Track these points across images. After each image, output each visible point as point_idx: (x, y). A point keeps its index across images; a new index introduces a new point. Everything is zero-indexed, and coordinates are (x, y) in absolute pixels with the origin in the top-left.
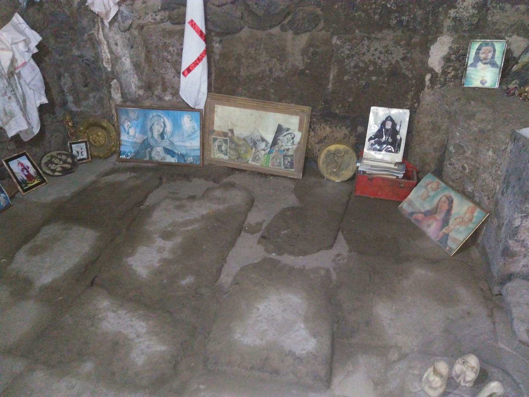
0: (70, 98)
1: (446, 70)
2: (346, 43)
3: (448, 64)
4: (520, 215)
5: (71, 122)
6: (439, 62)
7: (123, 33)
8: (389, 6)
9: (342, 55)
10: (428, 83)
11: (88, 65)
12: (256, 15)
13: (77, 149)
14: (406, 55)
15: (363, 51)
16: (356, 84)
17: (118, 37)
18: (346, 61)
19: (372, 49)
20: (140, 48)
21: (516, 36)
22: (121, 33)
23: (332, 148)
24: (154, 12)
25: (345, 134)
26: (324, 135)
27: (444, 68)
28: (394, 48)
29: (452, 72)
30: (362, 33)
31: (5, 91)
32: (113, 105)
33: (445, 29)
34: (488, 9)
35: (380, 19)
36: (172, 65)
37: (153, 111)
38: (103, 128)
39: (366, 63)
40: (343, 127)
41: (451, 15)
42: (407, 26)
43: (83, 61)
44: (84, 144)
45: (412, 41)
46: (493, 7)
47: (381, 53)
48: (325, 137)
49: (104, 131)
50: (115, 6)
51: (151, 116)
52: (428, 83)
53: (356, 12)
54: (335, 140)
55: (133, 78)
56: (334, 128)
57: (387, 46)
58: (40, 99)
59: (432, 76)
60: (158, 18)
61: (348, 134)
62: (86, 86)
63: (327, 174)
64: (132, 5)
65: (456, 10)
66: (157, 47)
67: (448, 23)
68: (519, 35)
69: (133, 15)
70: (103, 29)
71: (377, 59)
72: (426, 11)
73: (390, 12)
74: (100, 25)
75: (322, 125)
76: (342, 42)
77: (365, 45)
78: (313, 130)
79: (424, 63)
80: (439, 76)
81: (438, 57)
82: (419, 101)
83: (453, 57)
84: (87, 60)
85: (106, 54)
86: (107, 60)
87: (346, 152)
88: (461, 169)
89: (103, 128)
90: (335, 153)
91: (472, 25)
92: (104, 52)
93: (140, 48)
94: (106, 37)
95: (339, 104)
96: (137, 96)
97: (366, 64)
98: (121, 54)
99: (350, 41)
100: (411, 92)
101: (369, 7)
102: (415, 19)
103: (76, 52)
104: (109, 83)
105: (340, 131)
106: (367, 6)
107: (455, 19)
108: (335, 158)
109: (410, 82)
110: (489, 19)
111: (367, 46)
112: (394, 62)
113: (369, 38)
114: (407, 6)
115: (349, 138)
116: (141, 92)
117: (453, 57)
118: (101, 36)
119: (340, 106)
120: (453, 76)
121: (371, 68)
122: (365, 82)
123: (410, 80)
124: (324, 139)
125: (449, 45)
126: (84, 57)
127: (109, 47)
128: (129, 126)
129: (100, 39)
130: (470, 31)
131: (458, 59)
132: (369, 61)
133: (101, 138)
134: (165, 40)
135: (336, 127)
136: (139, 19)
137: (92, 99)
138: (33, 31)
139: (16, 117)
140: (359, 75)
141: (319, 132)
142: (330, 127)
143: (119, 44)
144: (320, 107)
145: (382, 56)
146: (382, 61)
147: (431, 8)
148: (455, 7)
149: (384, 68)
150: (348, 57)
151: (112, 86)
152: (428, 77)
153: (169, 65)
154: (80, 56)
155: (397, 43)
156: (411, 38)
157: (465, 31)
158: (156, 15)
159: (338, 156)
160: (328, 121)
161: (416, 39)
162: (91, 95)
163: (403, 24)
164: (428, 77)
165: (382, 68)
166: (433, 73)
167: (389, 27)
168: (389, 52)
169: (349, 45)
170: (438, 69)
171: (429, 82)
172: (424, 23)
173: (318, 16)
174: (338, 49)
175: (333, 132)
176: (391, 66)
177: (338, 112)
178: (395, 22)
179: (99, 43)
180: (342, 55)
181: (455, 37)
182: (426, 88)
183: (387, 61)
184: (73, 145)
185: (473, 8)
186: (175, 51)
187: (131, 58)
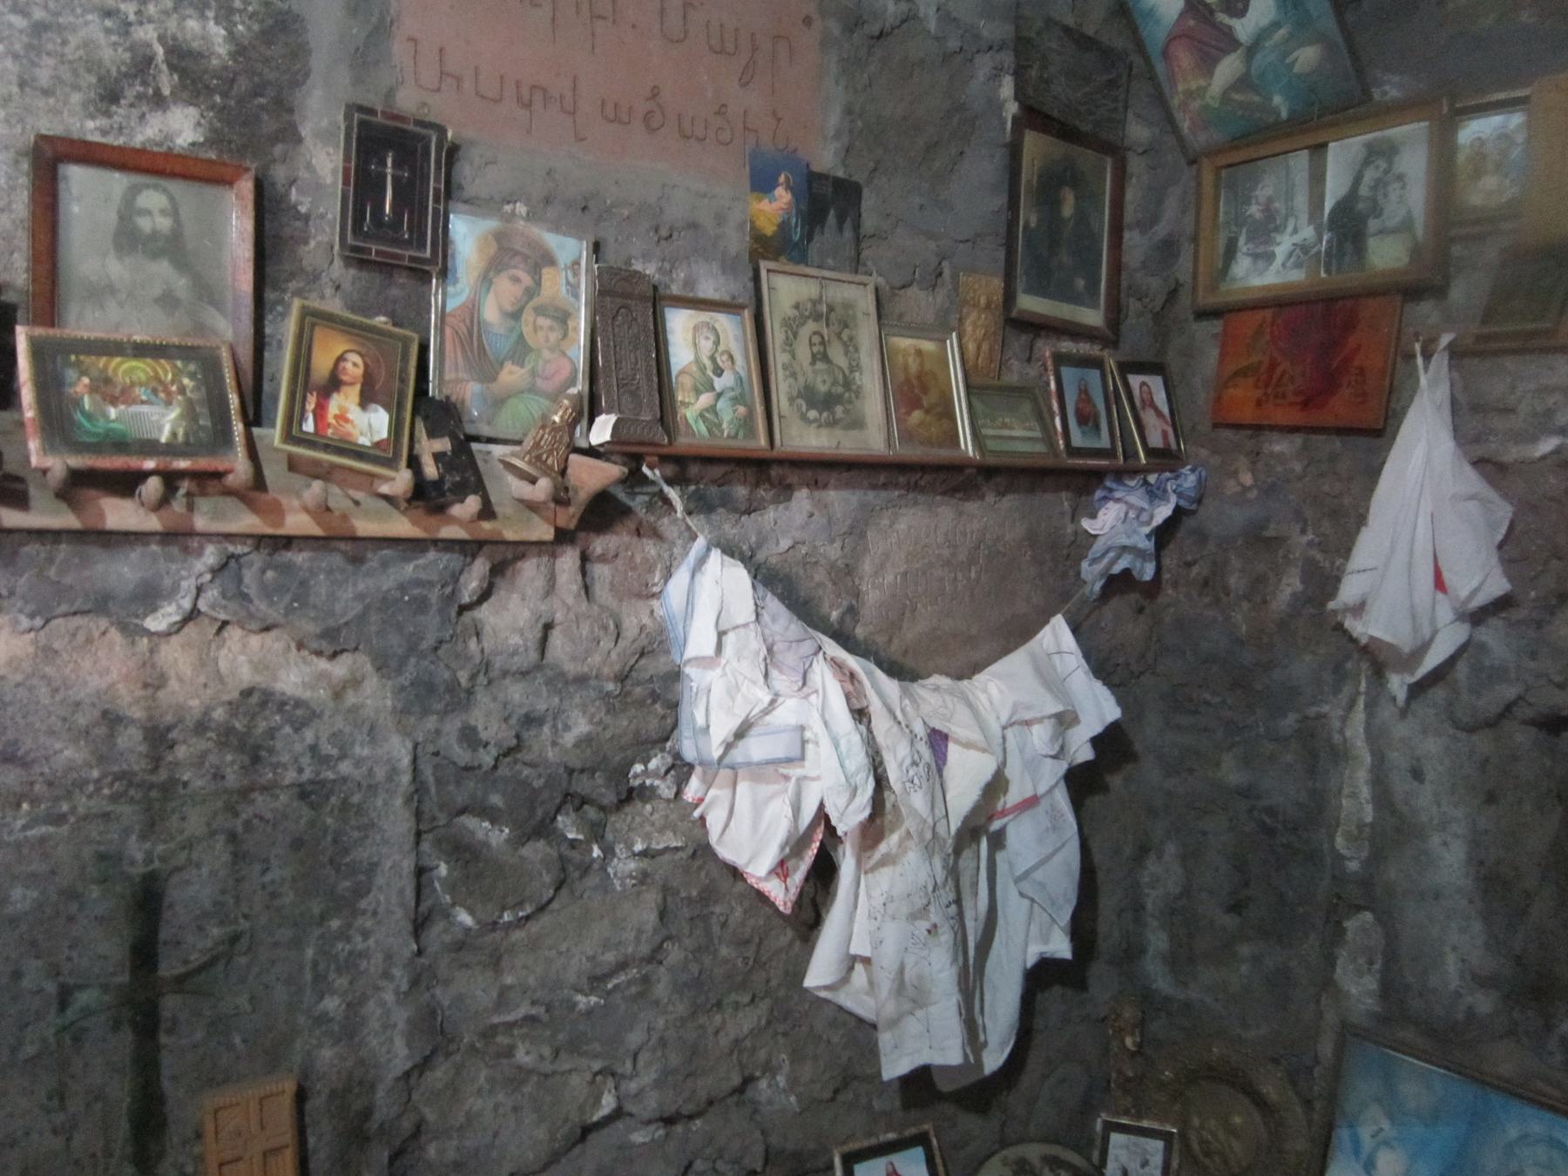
0: (1158, 940)
5: (1133, 1034)
7: (1462, 735)
11: (1270, 832)
13: (1124, 1157)
17: (1432, 746)
22: (1451, 731)
31: (925, 901)
32: (1330, 1018)
37: (1529, 1111)
38: (1258, 1105)
43: (1250, 811)
44: (1160, 1144)
49: (1257, 1117)
50: (1458, 623)
51: (1513, 1133)
58: (1045, 939)
62: (1236, 908)
64: (1539, 625)
69: (1532, 665)
70: (1370, 707)
74: (1363, 687)
84: (1270, 811)
89: (1260, 1103)
92: (1354, 795)
94: (1374, 736)
96: (1460, 1017)
98: (1431, 819)
103: (1232, 773)
104: (1339, 923)
116: (1484, 1003)
127: (1379, 779)
128: (1381, 1136)
129: (1345, 740)
133: (1236, 1145)
137: (1244, 969)
138: (1098, 686)
139: (932, 1009)
143: (1430, 775)
151: (1349, 936)
154: (1246, 792)
162: (1245, 950)
179: (1340, 755)
184: (1116, 1138)
187: (1475, 843)
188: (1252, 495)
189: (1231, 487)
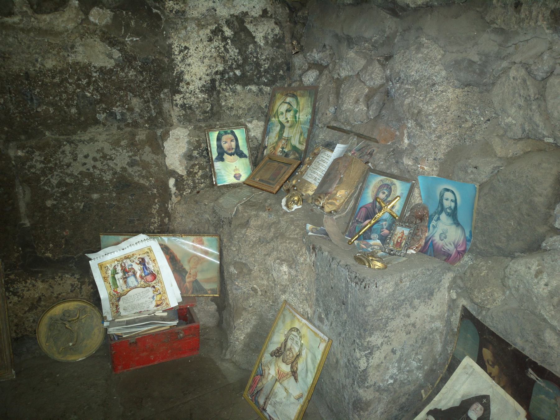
1: (191, 170)
2: (34, 152)
6: (180, 161)
8: (89, 95)
9: (33, 170)
10: (173, 189)
14: (133, 158)
15: (66, 161)
16: (70, 210)
18: (42, 178)
19: (80, 156)
21: (257, 121)
23: (58, 310)
25: (72, 285)
26: (37, 296)
27: (188, 168)
28: (113, 151)
29: (199, 171)
30: (57, 136)
33: (175, 120)
34: (219, 92)
35: (80, 113)
39: (77, 176)
40: (67, 276)
41: (178, 102)
42: (123, 120)
45: (137, 139)
46: (223, 89)
47: (95, 159)
48: (40, 299)
52: (173, 189)
53: (39, 105)
54: (57, 297)
56: (51, 281)
57: (103, 148)
59: (176, 181)
61: (77, 282)
63: (59, 353)
65: (182, 95)
68: (258, 119)
72: (143, 98)
75: (29, 281)
76: (27, 152)
77: (67, 152)
78: (15, 294)
79: (161, 166)
80: (185, 179)
81: (177, 155)
83: (195, 153)
87: (82, 310)
90: (66, 317)
91: (205, 112)
95: (49, 244)
99: (41, 148)
100: (155, 205)
101: (57, 99)
102: (131, 110)
105: (61, 282)
106: (54, 97)
107: (183, 106)
108: (67, 326)
109: (150, 192)
110: (223, 104)
111: (70, 153)
113: (70, 142)
114: (115, 93)
115: (81, 288)
117: (195, 153)
119: (51, 245)
120: (201, 176)
121: (87, 183)
122: (83, 203)
123: (148, 190)
124: (37, 302)
125: (186, 140)
131: (201, 155)
135: (53, 278)
140: (70, 196)
141: (26, 294)
142: (42, 282)
144: (16, 255)
145: (98, 164)
148: (179, 92)
149: (106, 181)
150: (44, 173)
152: (172, 182)
156: (134, 135)
157: (199, 121)
159: (69, 322)
160: (38, 272)
161: (141, 135)
163: (116, 118)
164: (172, 182)
167: (97, 122)
169: (39, 155)
170: (181, 170)
171: (175, 188)
172: (147, 115)
174: (24, 164)
175: (51, 286)
176: (116, 176)
177: (50, 255)
178: (103, 116)
180: (33, 170)
181: (190, 128)
182: (173, 196)
183: (109, 170)
185: (202, 91)
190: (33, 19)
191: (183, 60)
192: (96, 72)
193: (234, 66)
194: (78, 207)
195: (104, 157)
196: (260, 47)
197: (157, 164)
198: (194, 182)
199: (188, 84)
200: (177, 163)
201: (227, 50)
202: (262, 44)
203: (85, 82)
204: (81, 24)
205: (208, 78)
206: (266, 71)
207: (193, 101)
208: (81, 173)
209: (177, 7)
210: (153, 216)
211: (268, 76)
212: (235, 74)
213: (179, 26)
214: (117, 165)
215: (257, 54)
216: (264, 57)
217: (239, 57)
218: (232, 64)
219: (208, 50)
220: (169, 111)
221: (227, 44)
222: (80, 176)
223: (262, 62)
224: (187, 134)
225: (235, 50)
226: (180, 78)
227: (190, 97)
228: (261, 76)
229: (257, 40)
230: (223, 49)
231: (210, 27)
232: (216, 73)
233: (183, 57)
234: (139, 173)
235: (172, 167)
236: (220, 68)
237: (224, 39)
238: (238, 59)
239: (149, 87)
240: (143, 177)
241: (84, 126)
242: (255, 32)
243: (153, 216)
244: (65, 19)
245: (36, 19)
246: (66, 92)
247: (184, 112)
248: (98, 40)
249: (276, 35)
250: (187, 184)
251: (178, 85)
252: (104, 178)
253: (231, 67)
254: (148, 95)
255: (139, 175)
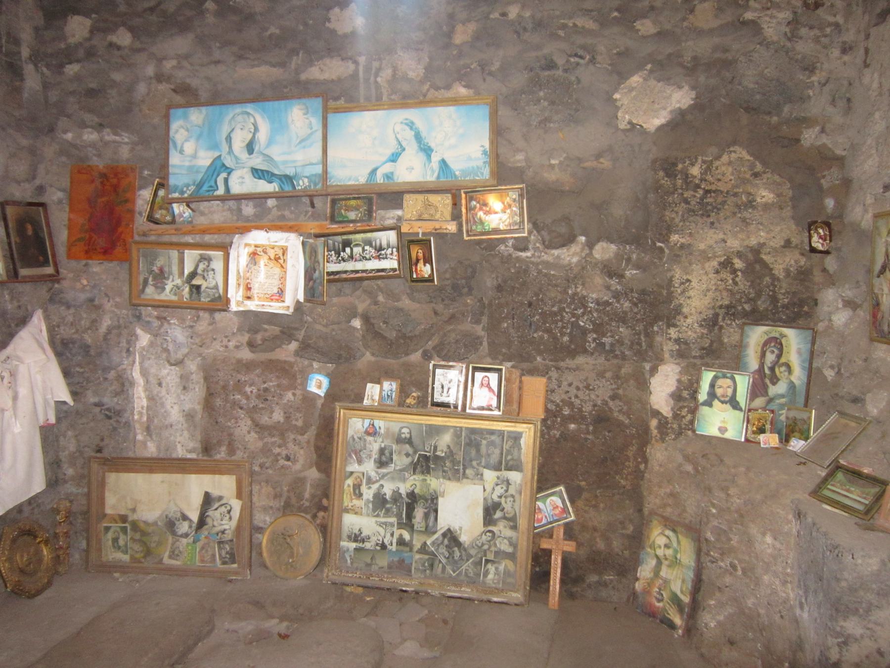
1: (678, 412)
3: (681, 404)
4: (836, 641)
6: (666, 401)
7: (173, 367)
8: (582, 324)
10: (655, 432)
12: (384, 338)
14: (616, 391)
19: (565, 383)
20: (197, 390)
24: (226, 337)
28: (597, 382)
29: (687, 415)
30: (547, 362)
33: (667, 355)
34: (721, 328)
35: (571, 341)
36: (247, 413)
41: (671, 336)
42: (612, 351)
43: (101, 411)
46: (727, 325)
47: (578, 389)
52: (655, 432)
53: (535, 331)
55: (181, 435)
60: (231, 344)
65: (677, 329)
66: (224, 388)
67: (669, 347)
71: (573, 398)
72: (634, 329)
73: (584, 332)
79: (644, 402)
80: (670, 422)
81: (664, 394)
82: (646, 461)
83: (685, 394)
84: (108, 409)
85: (140, 398)
86: (140, 409)
88: (729, 568)
91: (703, 349)
93: (197, 390)
94: (144, 373)
97: (557, 405)
107: (677, 341)
112: (599, 402)
113: (558, 368)
114: (607, 324)
117: (685, 394)
118: (136, 374)
121: (566, 411)
126: (103, 405)
127: (146, 389)
130: (701, 357)
132: (562, 401)
134: (239, 377)
136: (201, 346)
146: (581, 400)
147: (642, 327)
148: (675, 326)
152: (654, 423)
153: (241, 413)
155: (601, 375)
157: (695, 357)
158: (229, 341)
163: (604, 348)
164: (654, 423)
165: (582, 411)
166: (660, 417)
167: (585, 351)
168: (591, 387)
171: (656, 431)
173: (478, 338)
179: (132, 384)
183: (590, 400)
186: (254, 391)
188: (88, 288)
189: (78, 286)
190: (543, 254)
191: (683, 292)
192: (592, 303)
193: (743, 300)
194: (555, 435)
195: (587, 387)
196: (778, 279)
197: (640, 401)
198: (680, 426)
199: (686, 317)
200: (663, 403)
201: (735, 283)
202: (781, 277)
203: (580, 311)
204: (585, 258)
205: (712, 312)
206: (783, 306)
207: (691, 335)
208: (562, 401)
209: (682, 240)
210: (628, 459)
211: (787, 312)
212: (743, 308)
213: (683, 259)
214: (598, 396)
215: (776, 286)
216: (783, 291)
217: (751, 290)
218: (742, 298)
219: (713, 282)
220: (661, 345)
221: (737, 276)
222: (561, 404)
223: (781, 296)
224: (678, 371)
225: (746, 283)
226: (678, 311)
227: (687, 332)
228: (778, 313)
229: (776, 272)
230: (731, 281)
231: (718, 259)
232: (721, 307)
233: (684, 289)
234: (620, 408)
235: (656, 407)
236: (726, 302)
237: (734, 271)
238: (749, 292)
239: (643, 319)
240: (624, 414)
241: (573, 354)
242: (773, 264)
243: (628, 459)
244: (571, 253)
245: (546, 253)
246: (561, 321)
247: (678, 347)
248: (598, 272)
249: (801, 267)
250: (671, 427)
251: (675, 318)
252: (584, 409)
253: (739, 301)
254: (640, 327)
255: (619, 411)
